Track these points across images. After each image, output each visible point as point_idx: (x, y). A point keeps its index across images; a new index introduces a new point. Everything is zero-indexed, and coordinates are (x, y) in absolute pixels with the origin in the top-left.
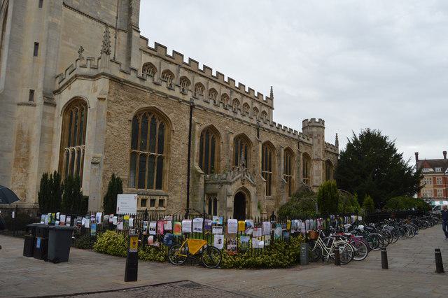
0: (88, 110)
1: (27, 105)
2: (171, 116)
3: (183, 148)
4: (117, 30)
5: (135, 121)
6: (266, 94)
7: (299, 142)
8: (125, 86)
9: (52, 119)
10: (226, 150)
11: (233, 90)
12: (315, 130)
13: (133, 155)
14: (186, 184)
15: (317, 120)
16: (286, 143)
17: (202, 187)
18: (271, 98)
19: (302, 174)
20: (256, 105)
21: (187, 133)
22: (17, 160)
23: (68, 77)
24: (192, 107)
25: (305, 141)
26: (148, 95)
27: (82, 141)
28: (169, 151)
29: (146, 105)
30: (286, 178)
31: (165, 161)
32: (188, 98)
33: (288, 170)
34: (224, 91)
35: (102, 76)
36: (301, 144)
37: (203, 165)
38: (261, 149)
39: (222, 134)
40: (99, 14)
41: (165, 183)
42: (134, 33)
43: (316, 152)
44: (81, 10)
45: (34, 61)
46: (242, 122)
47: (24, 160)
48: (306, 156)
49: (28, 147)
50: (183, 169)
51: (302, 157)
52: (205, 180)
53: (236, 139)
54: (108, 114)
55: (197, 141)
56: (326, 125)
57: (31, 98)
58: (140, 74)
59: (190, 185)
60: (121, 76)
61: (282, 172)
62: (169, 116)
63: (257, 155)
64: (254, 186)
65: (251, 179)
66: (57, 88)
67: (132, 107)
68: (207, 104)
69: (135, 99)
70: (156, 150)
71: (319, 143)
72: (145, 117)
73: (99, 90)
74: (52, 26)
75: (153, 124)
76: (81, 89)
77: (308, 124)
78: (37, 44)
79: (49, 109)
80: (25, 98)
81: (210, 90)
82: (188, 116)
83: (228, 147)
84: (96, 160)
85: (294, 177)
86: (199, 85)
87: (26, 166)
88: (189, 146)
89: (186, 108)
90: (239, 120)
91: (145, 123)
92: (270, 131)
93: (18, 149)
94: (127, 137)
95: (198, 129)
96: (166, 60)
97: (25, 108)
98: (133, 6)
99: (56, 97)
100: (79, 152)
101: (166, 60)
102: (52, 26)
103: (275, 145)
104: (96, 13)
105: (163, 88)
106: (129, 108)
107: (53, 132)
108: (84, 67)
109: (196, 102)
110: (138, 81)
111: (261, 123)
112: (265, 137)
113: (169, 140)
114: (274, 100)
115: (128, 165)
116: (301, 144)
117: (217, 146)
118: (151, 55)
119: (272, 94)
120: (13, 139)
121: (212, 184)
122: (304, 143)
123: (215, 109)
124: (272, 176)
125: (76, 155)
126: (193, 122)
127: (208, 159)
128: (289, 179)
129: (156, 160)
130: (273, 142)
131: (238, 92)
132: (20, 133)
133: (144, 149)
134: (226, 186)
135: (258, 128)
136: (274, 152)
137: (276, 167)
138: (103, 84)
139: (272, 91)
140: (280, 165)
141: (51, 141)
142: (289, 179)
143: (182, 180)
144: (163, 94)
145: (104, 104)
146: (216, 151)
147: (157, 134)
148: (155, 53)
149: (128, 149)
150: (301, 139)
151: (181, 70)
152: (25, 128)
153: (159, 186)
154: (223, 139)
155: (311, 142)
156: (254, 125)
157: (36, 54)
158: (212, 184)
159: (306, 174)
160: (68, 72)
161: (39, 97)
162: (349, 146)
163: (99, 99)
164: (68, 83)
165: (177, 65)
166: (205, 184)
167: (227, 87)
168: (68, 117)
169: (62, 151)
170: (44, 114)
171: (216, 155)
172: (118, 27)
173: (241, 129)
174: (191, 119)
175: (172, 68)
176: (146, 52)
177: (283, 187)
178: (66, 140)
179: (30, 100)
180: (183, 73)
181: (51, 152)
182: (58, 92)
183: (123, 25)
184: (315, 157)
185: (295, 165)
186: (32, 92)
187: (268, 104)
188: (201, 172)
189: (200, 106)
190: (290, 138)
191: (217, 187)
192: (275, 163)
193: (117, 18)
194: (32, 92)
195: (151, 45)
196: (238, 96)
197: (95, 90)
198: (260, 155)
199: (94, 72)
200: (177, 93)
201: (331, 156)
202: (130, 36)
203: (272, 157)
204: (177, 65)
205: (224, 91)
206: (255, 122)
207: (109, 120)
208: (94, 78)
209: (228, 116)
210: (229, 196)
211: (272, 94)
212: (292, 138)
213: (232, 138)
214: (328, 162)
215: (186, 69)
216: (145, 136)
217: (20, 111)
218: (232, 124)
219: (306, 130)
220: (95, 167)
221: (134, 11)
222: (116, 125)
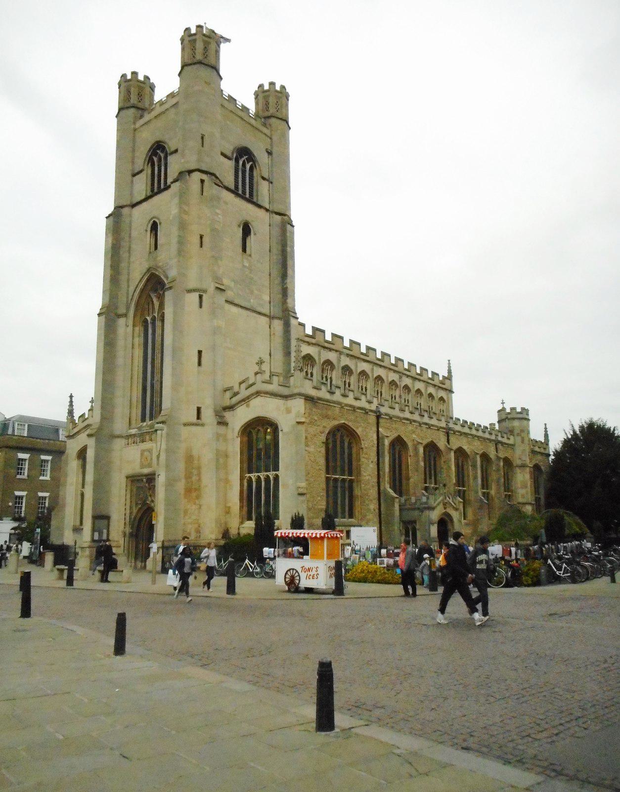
0: (281, 434)
1: (197, 425)
2: (359, 431)
3: (372, 467)
4: (271, 318)
5: (326, 443)
6: (443, 373)
7: (497, 443)
8: (317, 404)
9: (225, 440)
10: (415, 463)
11: (401, 374)
12: (516, 423)
13: (328, 479)
14: (377, 511)
15: (519, 410)
16: (482, 447)
17: (397, 513)
18: (449, 378)
19: (502, 488)
20: (431, 390)
21: (375, 449)
22: (188, 491)
23: (244, 393)
24: (378, 417)
25: (505, 440)
26: (337, 410)
27: (276, 468)
28: (359, 474)
29: (336, 423)
30: (484, 494)
31: (355, 485)
32: (373, 407)
33: (485, 484)
34: (393, 376)
35: (298, 396)
36: (500, 446)
37: (397, 487)
38: (453, 459)
39: (410, 444)
40: (253, 303)
41: (356, 512)
42: (293, 321)
43: (521, 455)
44: (236, 301)
45: (199, 372)
46: (429, 426)
47: (196, 490)
48: (508, 462)
49: (199, 474)
50: (373, 492)
51: (502, 464)
52: (400, 506)
53: (425, 447)
54: (306, 438)
55: (387, 459)
56: (531, 416)
57: (198, 417)
58: (343, 391)
59: (383, 513)
60: (313, 393)
61: (480, 487)
62: (358, 431)
63: (450, 467)
64: (456, 509)
65: (453, 502)
66: (227, 403)
67: (324, 427)
68: (392, 410)
69: (327, 417)
70: (347, 473)
71: (523, 442)
72: (334, 435)
73: (294, 411)
74: (216, 331)
75: (342, 442)
76: (262, 407)
77: (505, 417)
78: (200, 352)
79: (222, 430)
80: (194, 419)
81: (376, 378)
82: (375, 429)
83: (418, 461)
84: (301, 491)
85: (493, 492)
86: (363, 373)
87: (198, 497)
88: (378, 464)
89: (372, 418)
90: (426, 424)
91: (335, 442)
92: (462, 434)
93: (188, 476)
94: (322, 461)
95: (387, 442)
96: (324, 347)
97: (193, 428)
98: (289, 286)
99: (228, 415)
100: (267, 479)
101: (324, 347)
102: (216, 331)
103: (468, 451)
104: (249, 301)
105: (350, 400)
106: (321, 428)
107: (227, 456)
108: (269, 382)
109: (383, 410)
110: (328, 396)
111: (451, 425)
112: (456, 443)
113: (359, 460)
114: (454, 379)
115: (324, 493)
116: (500, 446)
117: (403, 459)
118: (309, 343)
119: (450, 372)
120: (181, 466)
121: (408, 509)
122: (503, 444)
123: (401, 415)
124: (467, 493)
125: (263, 483)
126: (380, 436)
127: (398, 481)
128: (487, 495)
129: (347, 485)
130: (465, 447)
131: (408, 376)
132: (189, 459)
133: (335, 473)
134: (427, 512)
135: (448, 432)
136: (467, 461)
137: (471, 481)
138: (299, 405)
139: (449, 367)
140: (475, 478)
141: (226, 466)
142: (487, 495)
143: (373, 506)
144: (350, 406)
145: (302, 428)
146: (404, 467)
147: (346, 454)
148: (313, 341)
149: (323, 475)
150: (500, 439)
151: (343, 357)
152: (195, 453)
153: (351, 516)
154: (411, 451)
155: (511, 442)
156: (444, 428)
157: (200, 364)
158: (408, 509)
159: (508, 486)
160: (243, 386)
161: (208, 415)
162: (567, 443)
163: (298, 423)
164: (246, 400)
165: (336, 351)
166: (400, 510)
167: (395, 371)
168: (245, 439)
169: (242, 479)
170: (218, 436)
171: (404, 472)
172: (272, 314)
173: (428, 437)
174: (378, 432)
175: (332, 356)
176: (304, 342)
177: (481, 508)
178: (245, 465)
179: (198, 417)
180: (345, 361)
181: (227, 481)
182: (231, 408)
183: (277, 311)
184: (519, 462)
185: (494, 476)
186: (199, 409)
187: (445, 385)
188: (395, 495)
189: (386, 414)
190: (484, 439)
191: (416, 513)
192: (468, 476)
193: (270, 303)
194: (199, 409)
195: (309, 331)
196: (407, 381)
197: (288, 411)
198: (453, 468)
199: (285, 391)
200: (363, 403)
201: (539, 457)
202: (287, 325)
203: (465, 467)
204: (336, 351)
205: (393, 376)
206: (443, 424)
207: (307, 445)
208: (286, 397)
209: (415, 421)
210: (433, 524)
211: (450, 372)
212: (488, 439)
213: (421, 450)
214: (537, 468)
215: (348, 355)
216: (335, 456)
217: (185, 432)
218: (418, 430)
219: (504, 424)
220: (302, 498)
221: (289, 292)
222: (312, 449)
